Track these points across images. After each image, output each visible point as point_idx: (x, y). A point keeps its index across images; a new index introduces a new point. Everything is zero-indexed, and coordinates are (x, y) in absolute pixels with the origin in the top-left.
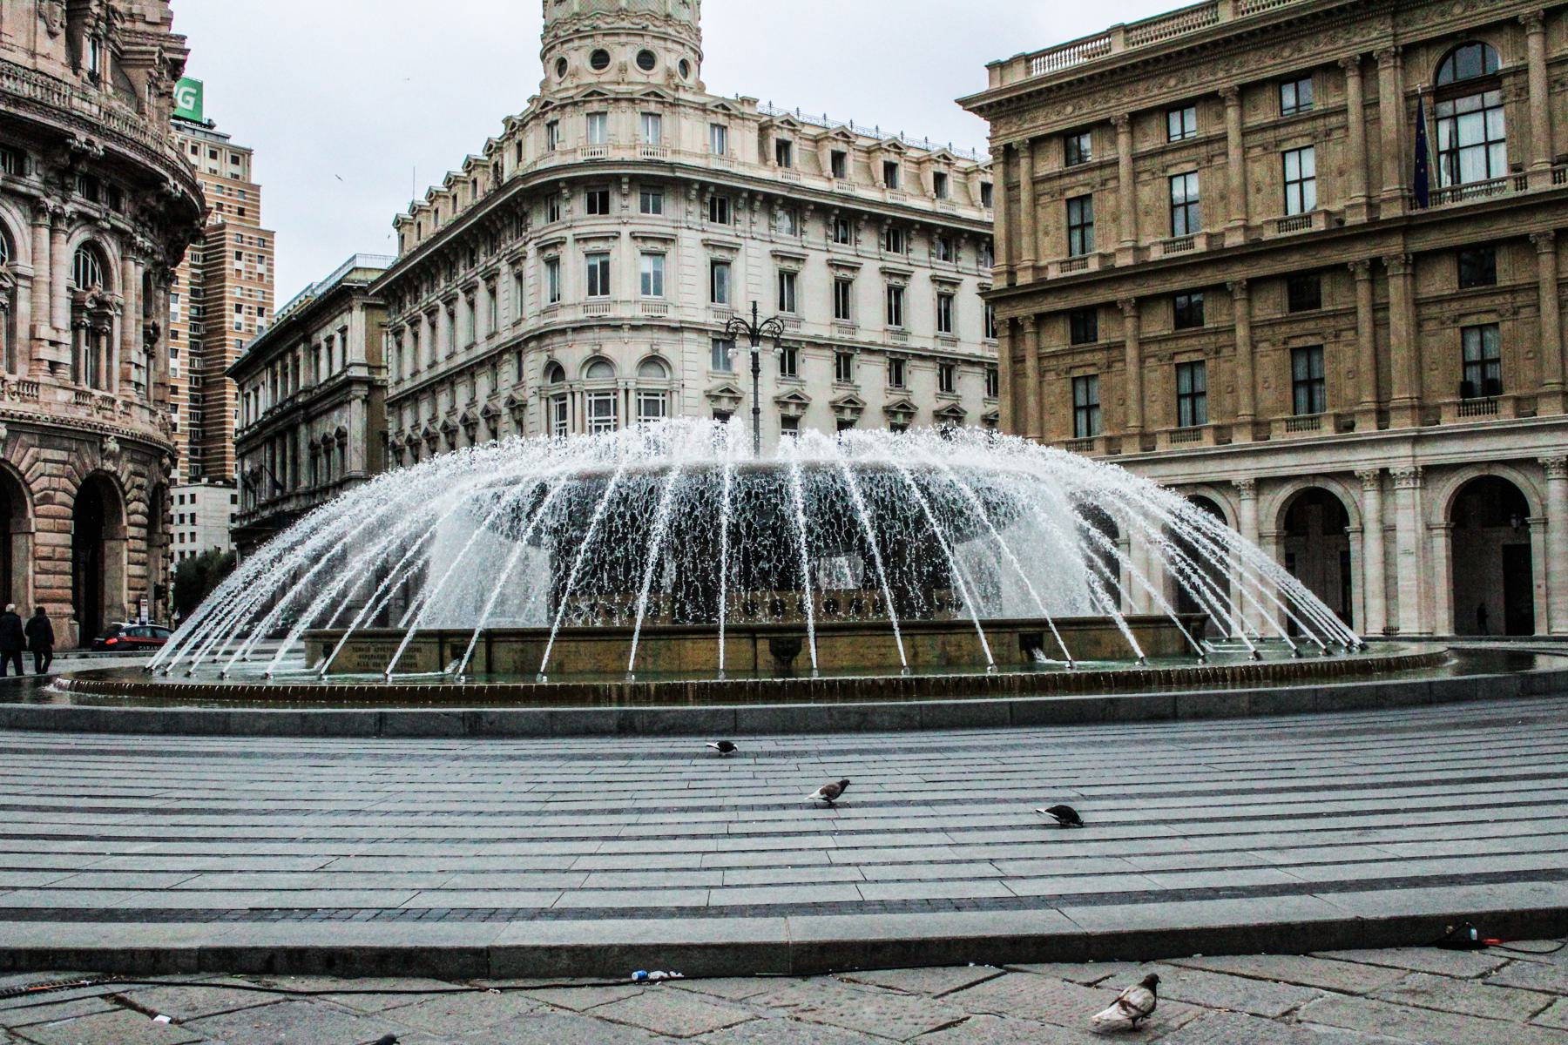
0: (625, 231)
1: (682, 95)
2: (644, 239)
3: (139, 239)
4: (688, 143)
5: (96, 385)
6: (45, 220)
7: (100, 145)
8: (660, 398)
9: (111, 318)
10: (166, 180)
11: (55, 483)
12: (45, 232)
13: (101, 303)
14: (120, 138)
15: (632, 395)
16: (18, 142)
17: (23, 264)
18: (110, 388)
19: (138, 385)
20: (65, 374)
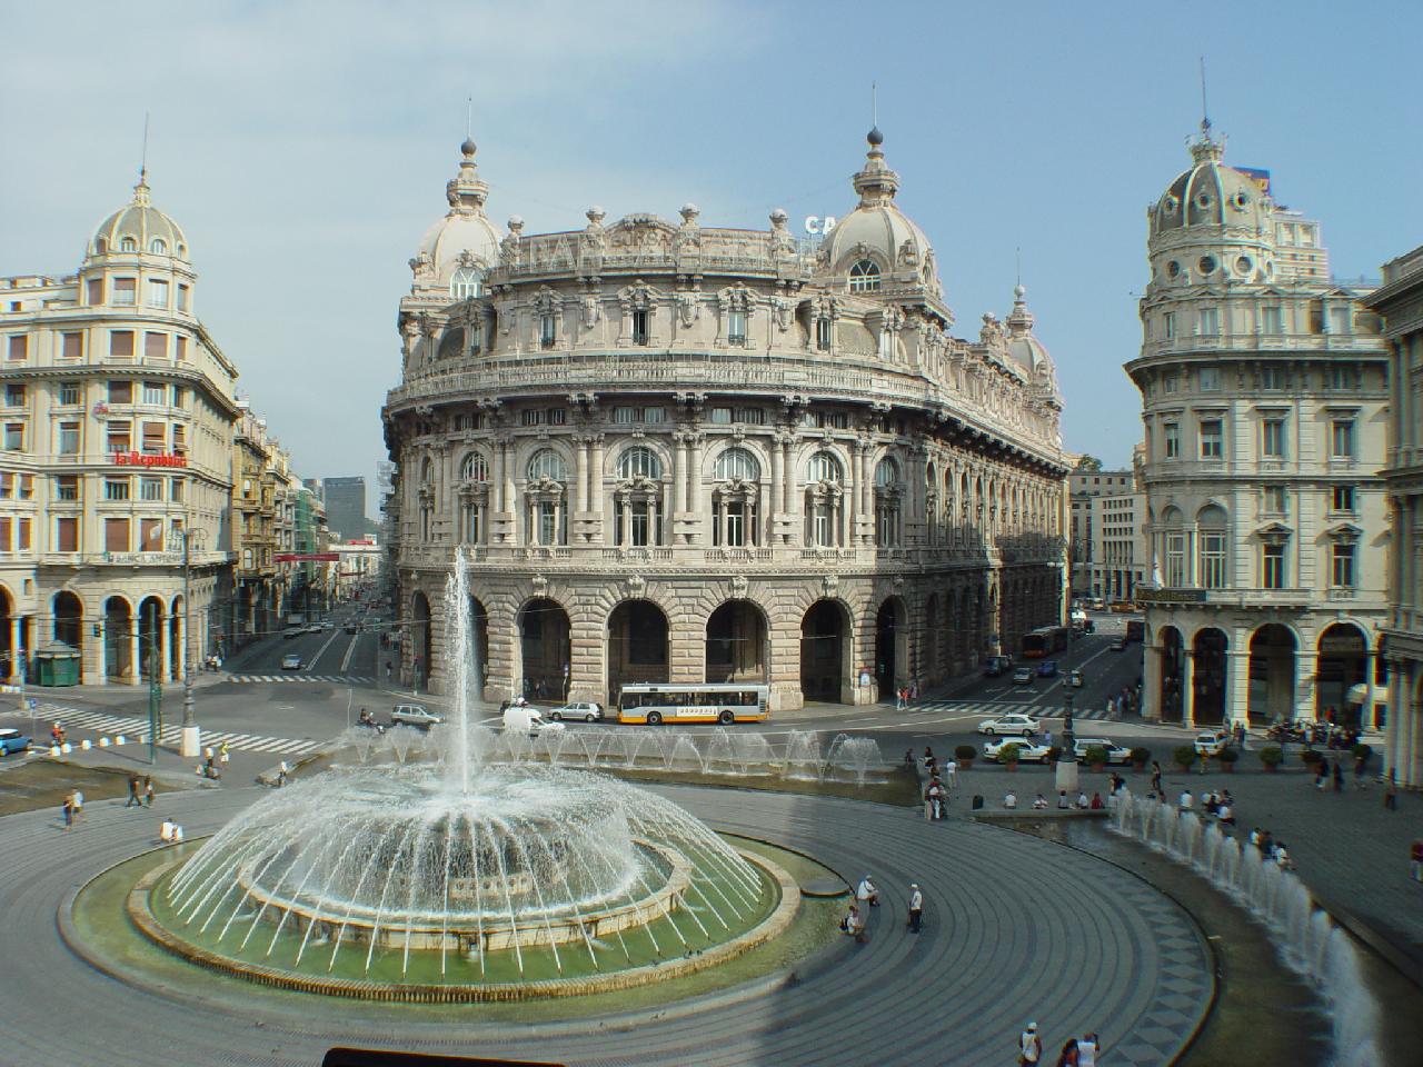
0: (1188, 405)
1: (1234, 290)
2: (1202, 411)
3: (862, 442)
4: (1240, 330)
5: (830, 543)
6: (780, 447)
7: (805, 398)
8: (1221, 537)
9: (842, 498)
10: (872, 403)
11: (787, 609)
12: (780, 456)
13: (830, 490)
14: (813, 390)
15: (1195, 536)
16: (754, 405)
17: (766, 477)
18: (841, 545)
19: (864, 536)
20: (798, 540)
